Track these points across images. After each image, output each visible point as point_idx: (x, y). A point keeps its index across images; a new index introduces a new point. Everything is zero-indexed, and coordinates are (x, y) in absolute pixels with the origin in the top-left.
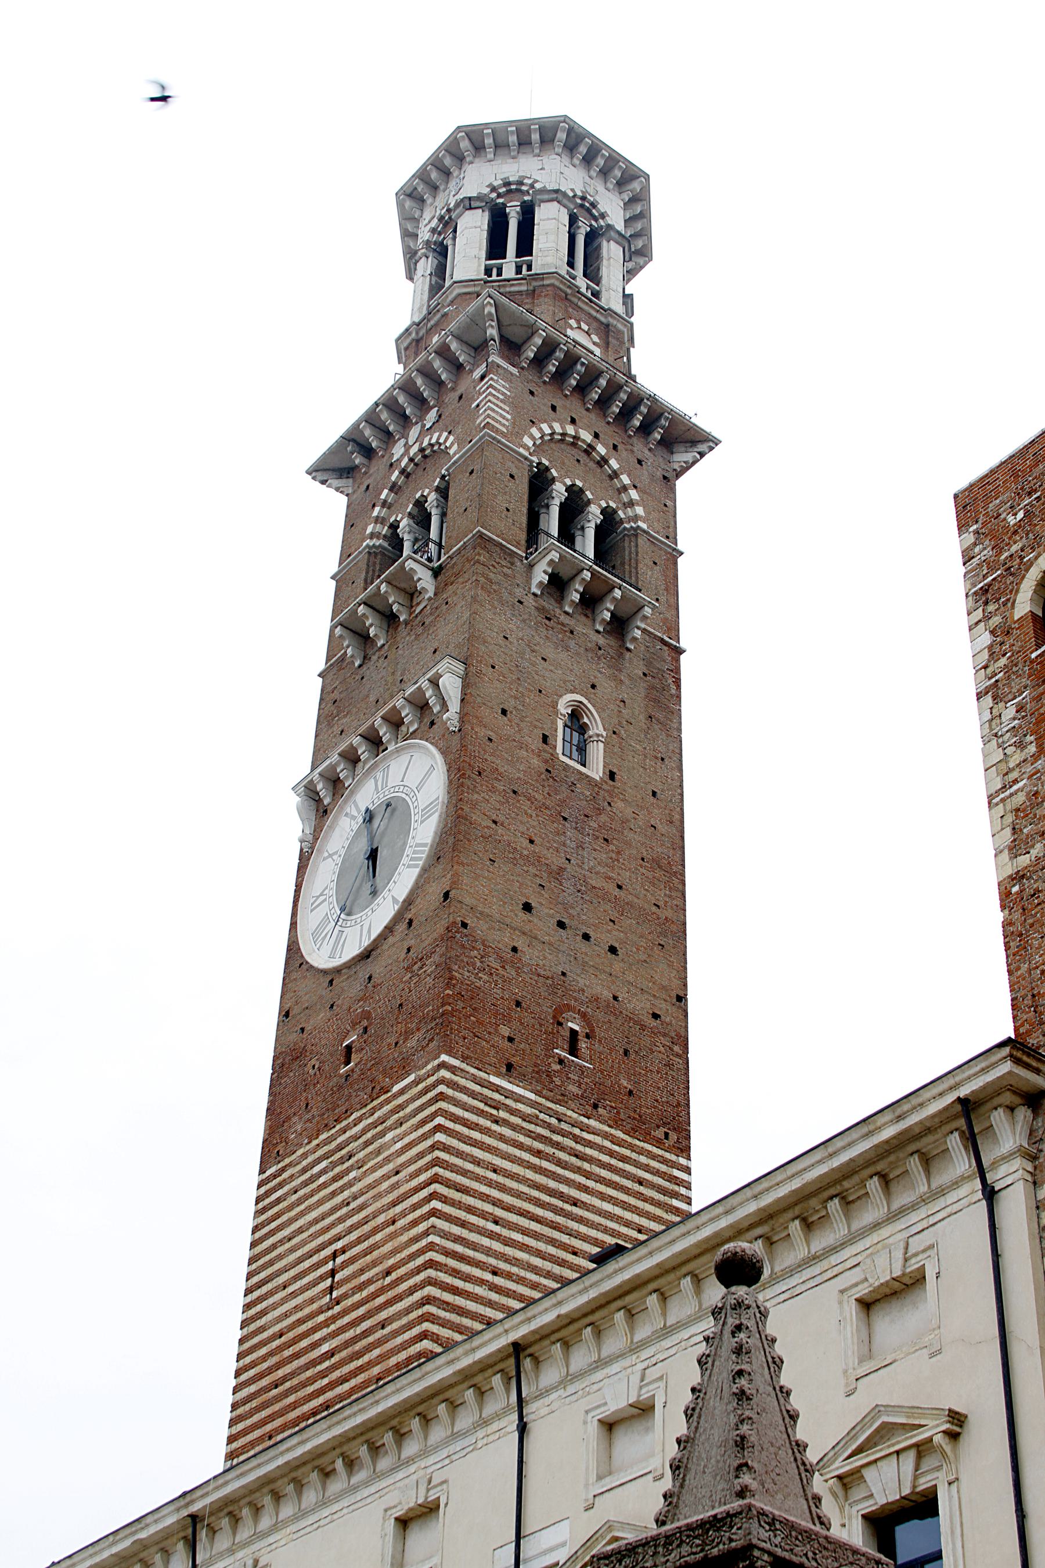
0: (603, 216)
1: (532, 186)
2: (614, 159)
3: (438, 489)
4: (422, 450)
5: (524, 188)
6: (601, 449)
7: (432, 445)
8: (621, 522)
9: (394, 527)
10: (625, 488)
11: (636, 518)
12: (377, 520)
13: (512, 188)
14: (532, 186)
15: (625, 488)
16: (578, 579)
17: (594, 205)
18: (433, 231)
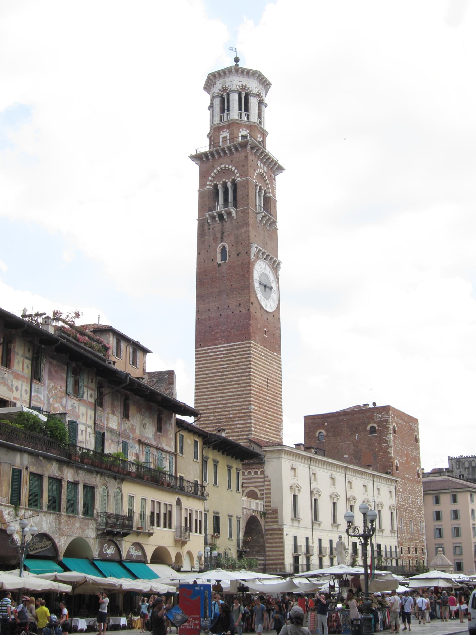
0: (262, 97)
1: (248, 88)
2: (266, 80)
3: (230, 182)
4: (225, 167)
5: (246, 88)
6: (265, 174)
7: (228, 168)
8: (266, 193)
9: (216, 186)
10: (267, 184)
11: (269, 193)
12: (211, 181)
13: (244, 88)
14: (248, 88)
16: (266, 218)
17: (260, 94)
18: (220, 90)
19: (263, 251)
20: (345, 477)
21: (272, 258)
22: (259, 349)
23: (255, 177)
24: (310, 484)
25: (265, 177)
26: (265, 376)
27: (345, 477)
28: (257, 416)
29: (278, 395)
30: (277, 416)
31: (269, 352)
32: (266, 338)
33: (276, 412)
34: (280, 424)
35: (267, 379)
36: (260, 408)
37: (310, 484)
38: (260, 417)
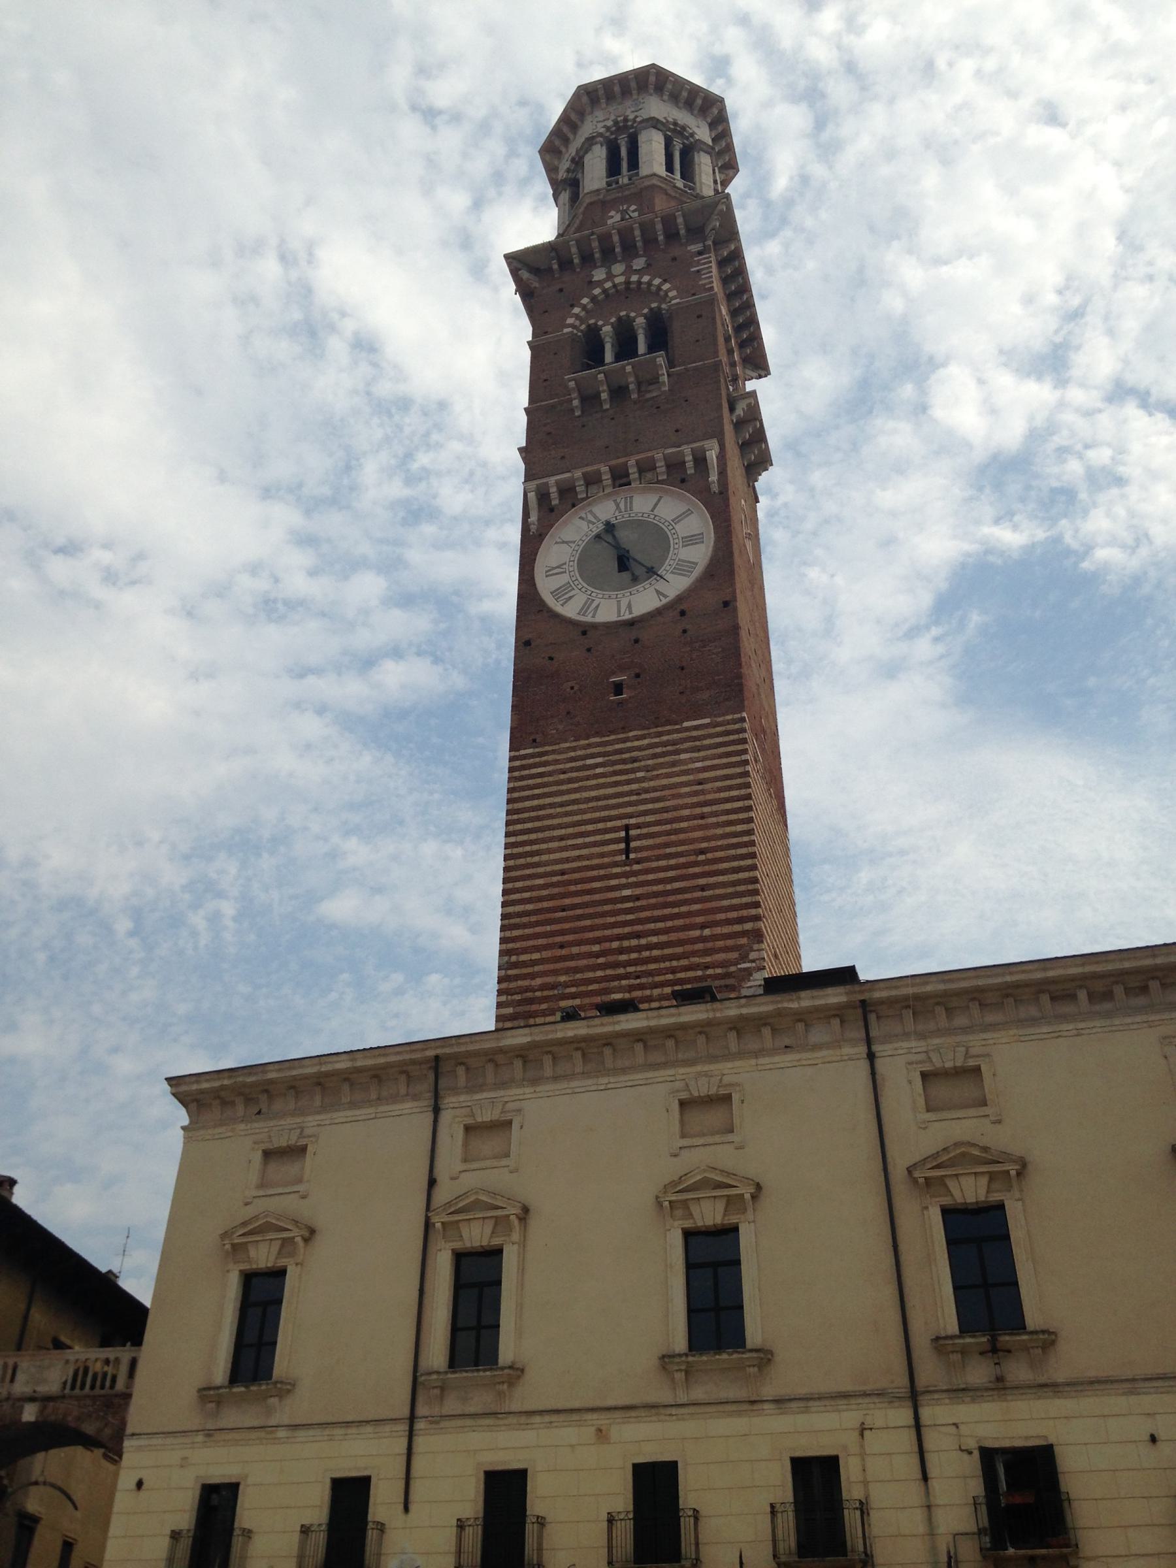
0: (634, 120)
15: (659, 288)
17: (626, 120)
19: (578, 474)
20: (871, 1056)
21: (646, 468)
22: (573, 754)
23: (570, 321)
24: (432, 1182)
25: (639, 283)
26: (610, 824)
27: (871, 1056)
28: (538, 981)
29: (710, 856)
30: (707, 932)
31: (637, 738)
32: (620, 703)
33: (699, 920)
34: (735, 955)
35: (627, 828)
36: (562, 946)
37: (432, 1182)
38: (563, 979)
